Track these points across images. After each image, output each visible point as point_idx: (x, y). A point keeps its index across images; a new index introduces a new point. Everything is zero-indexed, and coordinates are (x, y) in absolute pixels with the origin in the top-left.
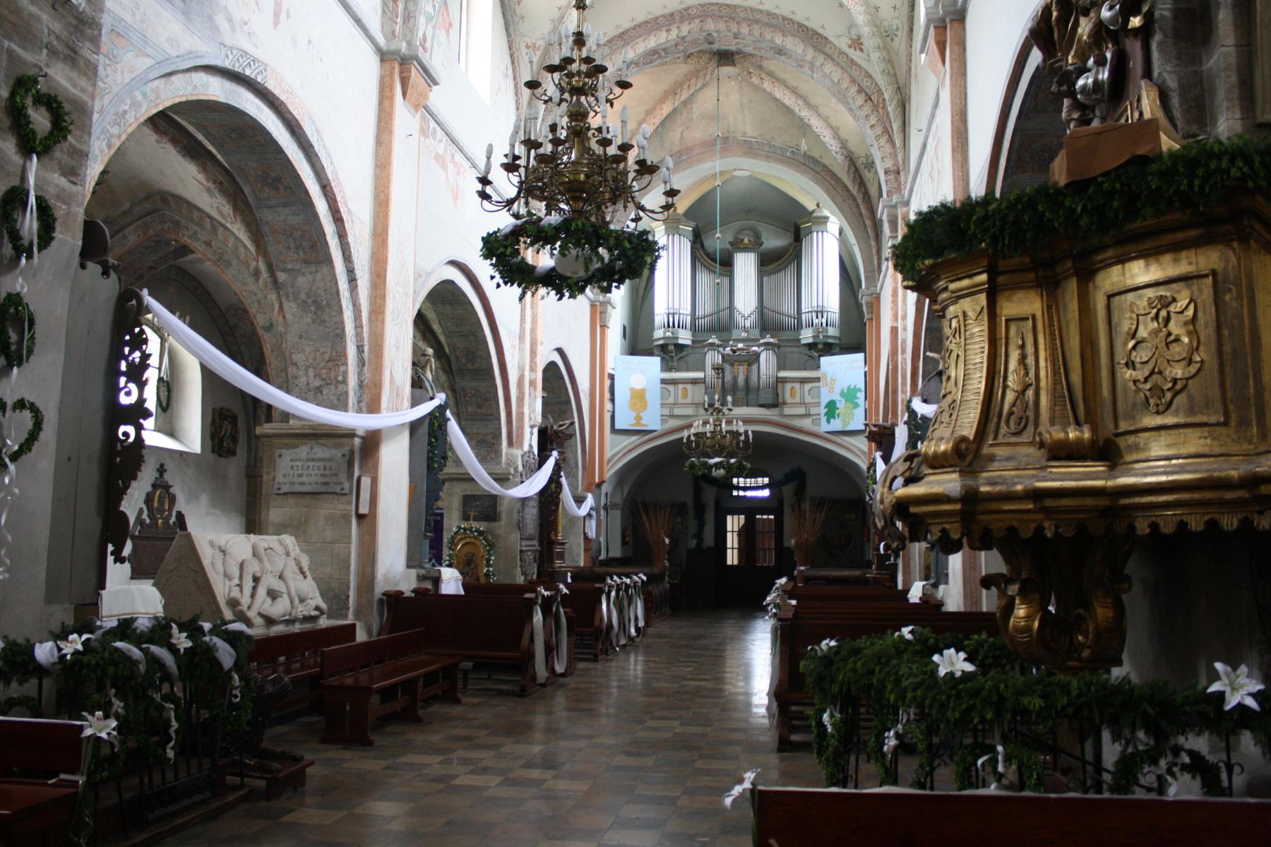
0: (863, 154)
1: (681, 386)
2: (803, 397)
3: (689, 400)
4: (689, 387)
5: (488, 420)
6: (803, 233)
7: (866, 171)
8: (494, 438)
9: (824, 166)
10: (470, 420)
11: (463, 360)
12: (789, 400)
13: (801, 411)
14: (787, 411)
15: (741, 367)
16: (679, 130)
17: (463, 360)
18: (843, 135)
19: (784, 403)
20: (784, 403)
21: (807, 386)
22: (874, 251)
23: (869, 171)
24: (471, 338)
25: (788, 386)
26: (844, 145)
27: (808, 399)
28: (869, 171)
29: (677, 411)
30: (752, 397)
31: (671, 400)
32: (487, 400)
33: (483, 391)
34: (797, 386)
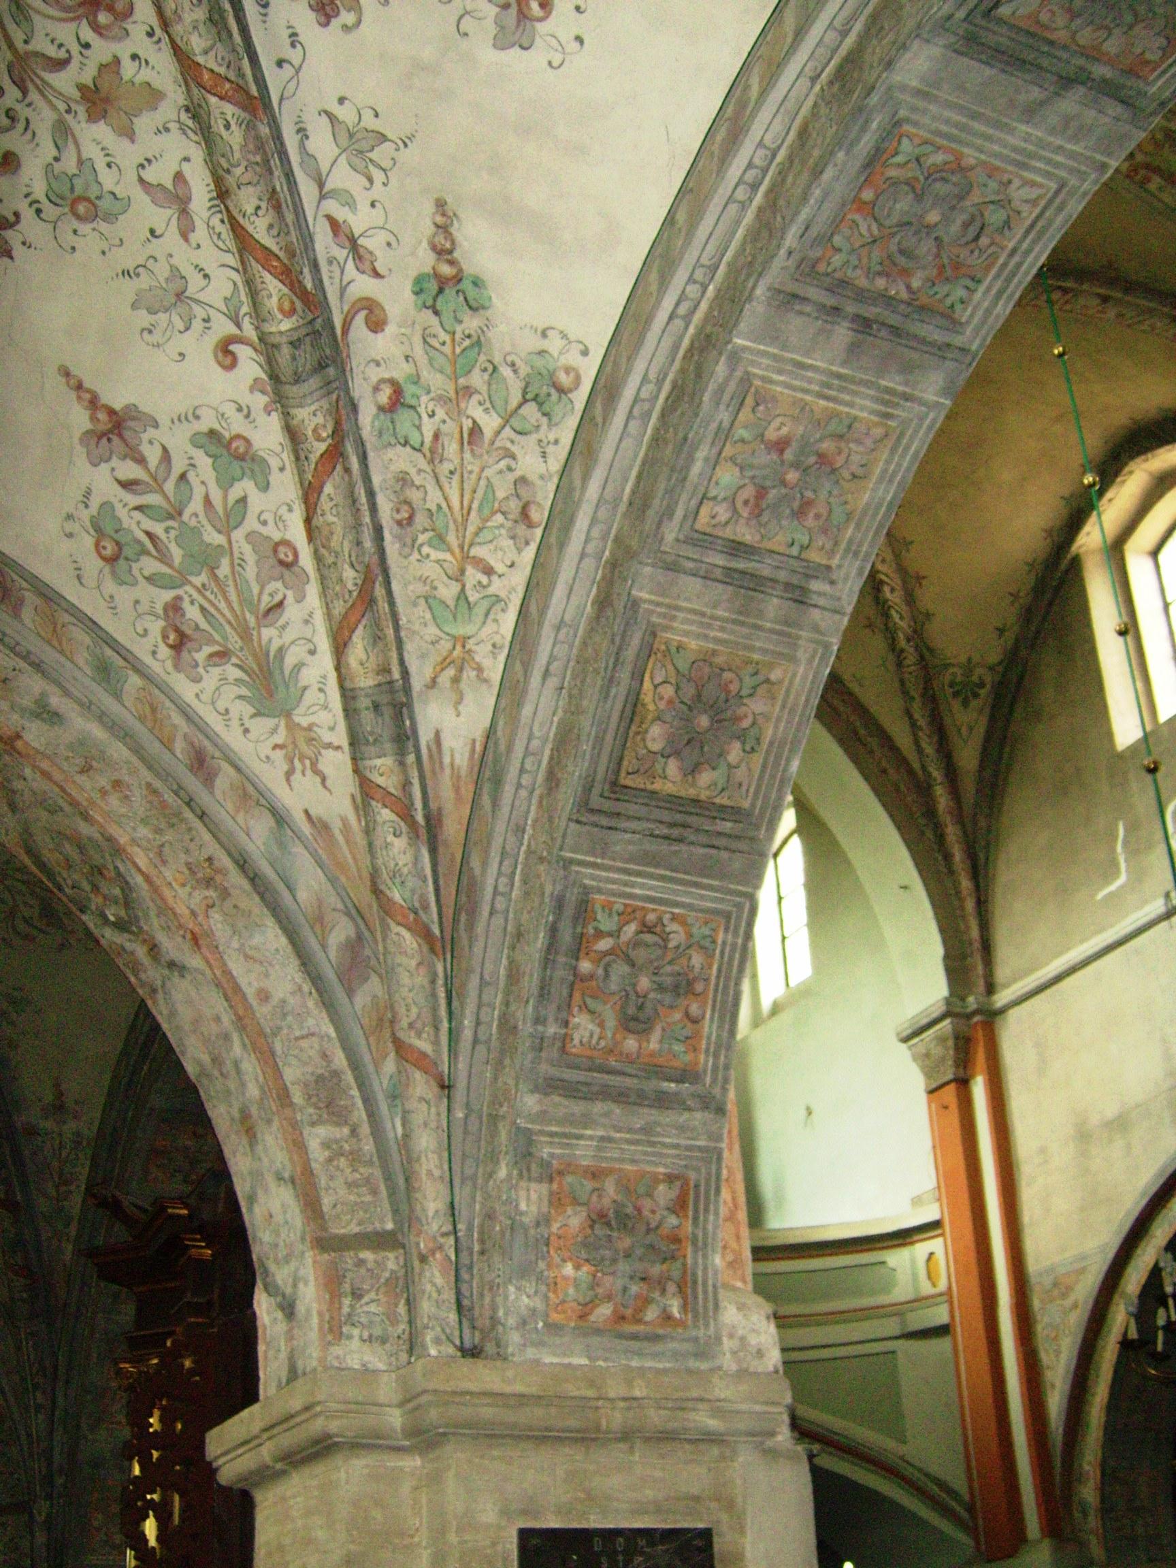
0: (963, 659)
5: (663, 1101)
7: (956, 705)
8: (679, 1206)
10: (571, 1091)
11: (656, 737)
17: (656, 737)
22: (970, 905)
23: (965, 703)
24: (774, 605)
28: (965, 703)
32: (684, 986)
33: (677, 936)
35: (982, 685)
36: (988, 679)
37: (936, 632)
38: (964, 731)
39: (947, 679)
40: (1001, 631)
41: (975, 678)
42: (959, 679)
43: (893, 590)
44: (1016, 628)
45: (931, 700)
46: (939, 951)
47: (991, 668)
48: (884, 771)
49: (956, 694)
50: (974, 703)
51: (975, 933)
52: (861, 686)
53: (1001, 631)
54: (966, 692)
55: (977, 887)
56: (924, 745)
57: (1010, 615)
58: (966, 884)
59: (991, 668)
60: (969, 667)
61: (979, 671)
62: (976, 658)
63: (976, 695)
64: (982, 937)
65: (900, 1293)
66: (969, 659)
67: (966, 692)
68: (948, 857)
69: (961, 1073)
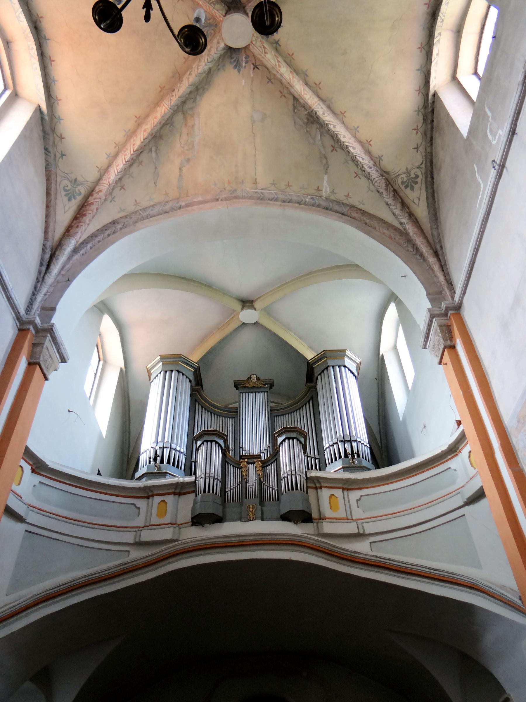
1: (157, 500)
2: (349, 509)
3: (167, 519)
4: (170, 499)
6: (317, 372)
7: (408, 191)
9: (352, 207)
12: (327, 512)
13: (350, 528)
14: (328, 528)
15: (251, 467)
16: (177, 162)
18: (376, 150)
19: (321, 518)
20: (321, 518)
21: (354, 495)
22: (436, 268)
23: (412, 189)
25: (325, 493)
26: (377, 162)
27: (357, 513)
28: (412, 189)
29: (147, 536)
30: (269, 507)
31: (140, 522)
34: (338, 493)
35: (417, 177)
36: (419, 174)
37: (388, 164)
38: (416, 201)
39: (400, 181)
40: (417, 148)
41: (413, 176)
42: (405, 179)
43: (354, 148)
44: (424, 143)
45: (396, 194)
46: (424, 292)
47: (419, 168)
48: (384, 233)
49: (406, 187)
50: (416, 187)
51: (441, 278)
52: (364, 204)
53: (417, 148)
54: (411, 183)
55: (439, 260)
56: (394, 211)
57: (417, 138)
58: (432, 260)
59: (419, 168)
60: (408, 172)
61: (412, 173)
62: (410, 167)
63: (416, 183)
64: (446, 280)
65: (460, 483)
66: (407, 169)
67: (411, 183)
68: (422, 255)
69: (449, 343)
